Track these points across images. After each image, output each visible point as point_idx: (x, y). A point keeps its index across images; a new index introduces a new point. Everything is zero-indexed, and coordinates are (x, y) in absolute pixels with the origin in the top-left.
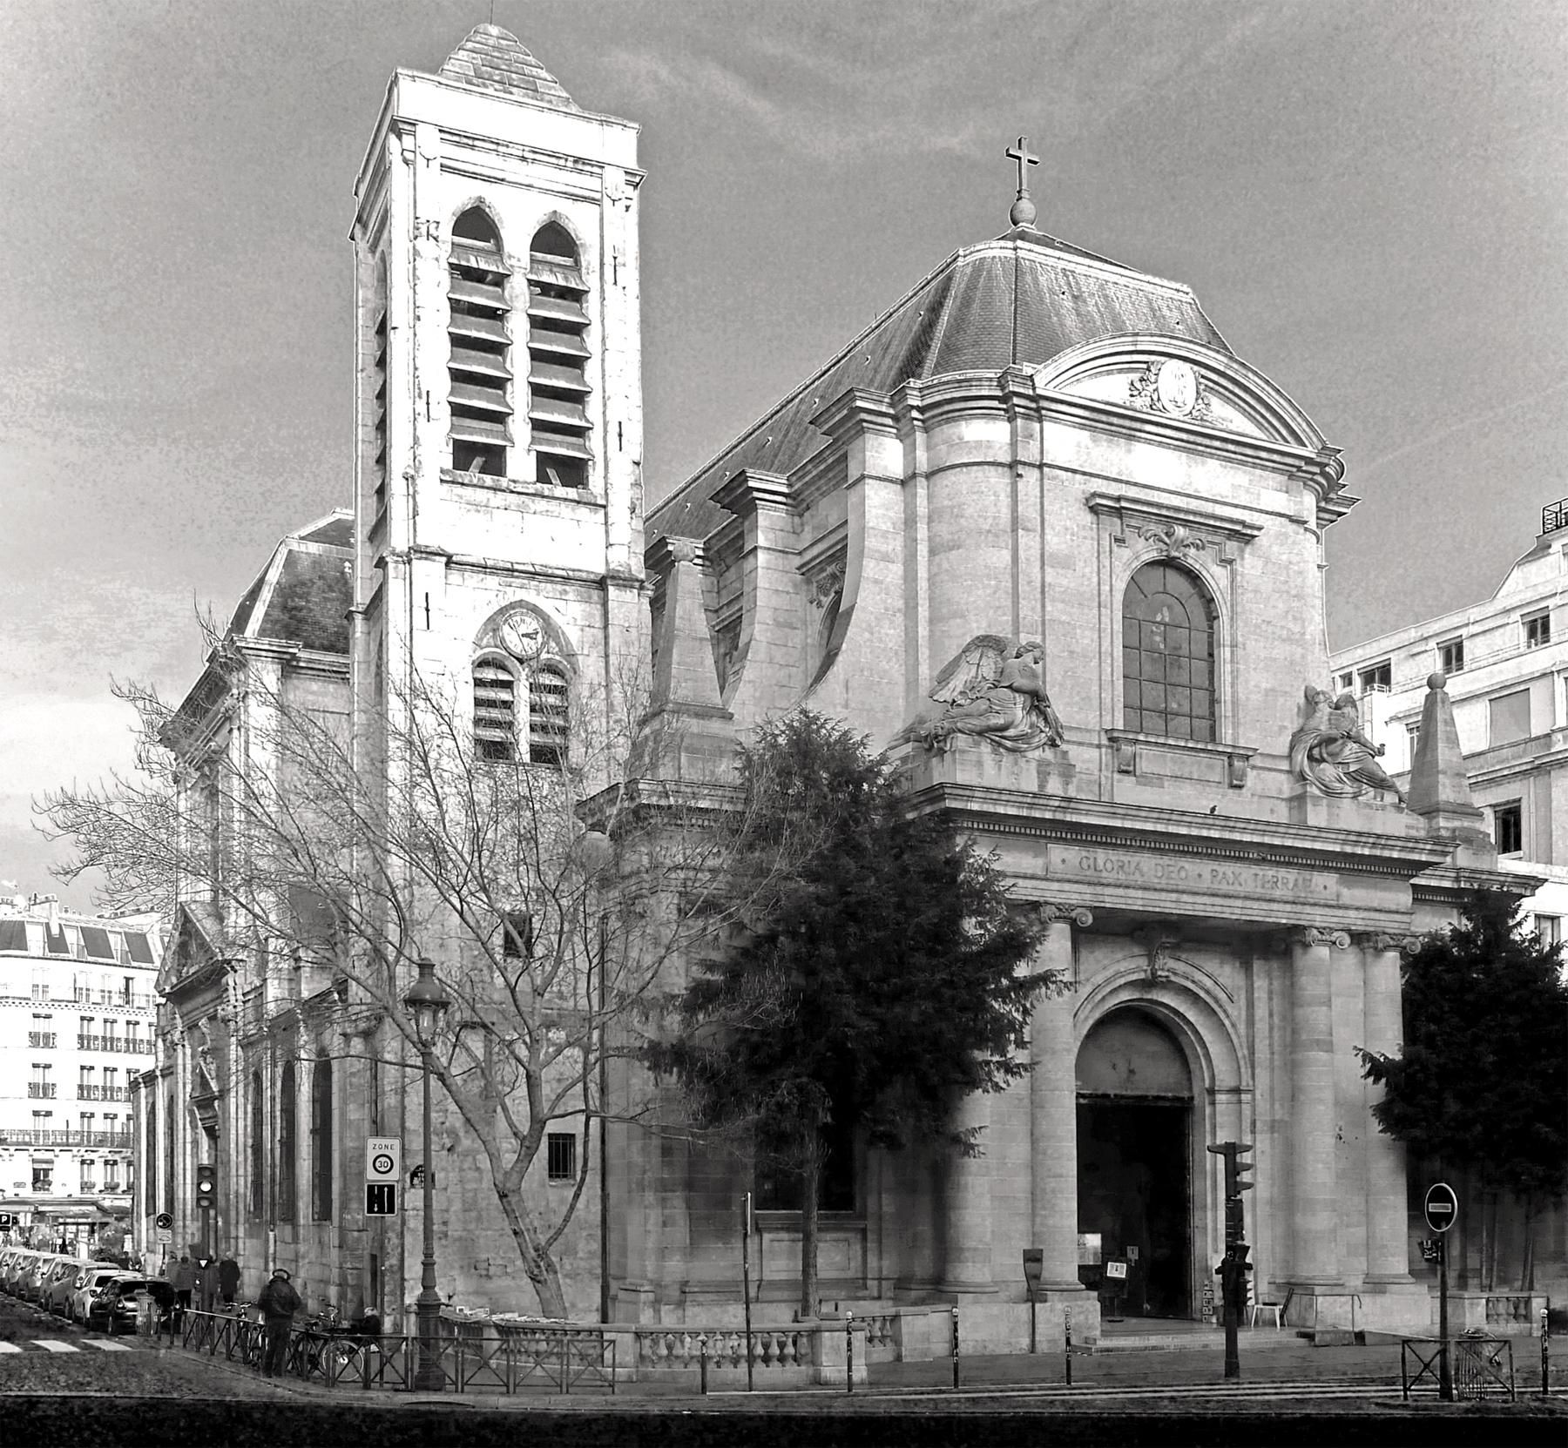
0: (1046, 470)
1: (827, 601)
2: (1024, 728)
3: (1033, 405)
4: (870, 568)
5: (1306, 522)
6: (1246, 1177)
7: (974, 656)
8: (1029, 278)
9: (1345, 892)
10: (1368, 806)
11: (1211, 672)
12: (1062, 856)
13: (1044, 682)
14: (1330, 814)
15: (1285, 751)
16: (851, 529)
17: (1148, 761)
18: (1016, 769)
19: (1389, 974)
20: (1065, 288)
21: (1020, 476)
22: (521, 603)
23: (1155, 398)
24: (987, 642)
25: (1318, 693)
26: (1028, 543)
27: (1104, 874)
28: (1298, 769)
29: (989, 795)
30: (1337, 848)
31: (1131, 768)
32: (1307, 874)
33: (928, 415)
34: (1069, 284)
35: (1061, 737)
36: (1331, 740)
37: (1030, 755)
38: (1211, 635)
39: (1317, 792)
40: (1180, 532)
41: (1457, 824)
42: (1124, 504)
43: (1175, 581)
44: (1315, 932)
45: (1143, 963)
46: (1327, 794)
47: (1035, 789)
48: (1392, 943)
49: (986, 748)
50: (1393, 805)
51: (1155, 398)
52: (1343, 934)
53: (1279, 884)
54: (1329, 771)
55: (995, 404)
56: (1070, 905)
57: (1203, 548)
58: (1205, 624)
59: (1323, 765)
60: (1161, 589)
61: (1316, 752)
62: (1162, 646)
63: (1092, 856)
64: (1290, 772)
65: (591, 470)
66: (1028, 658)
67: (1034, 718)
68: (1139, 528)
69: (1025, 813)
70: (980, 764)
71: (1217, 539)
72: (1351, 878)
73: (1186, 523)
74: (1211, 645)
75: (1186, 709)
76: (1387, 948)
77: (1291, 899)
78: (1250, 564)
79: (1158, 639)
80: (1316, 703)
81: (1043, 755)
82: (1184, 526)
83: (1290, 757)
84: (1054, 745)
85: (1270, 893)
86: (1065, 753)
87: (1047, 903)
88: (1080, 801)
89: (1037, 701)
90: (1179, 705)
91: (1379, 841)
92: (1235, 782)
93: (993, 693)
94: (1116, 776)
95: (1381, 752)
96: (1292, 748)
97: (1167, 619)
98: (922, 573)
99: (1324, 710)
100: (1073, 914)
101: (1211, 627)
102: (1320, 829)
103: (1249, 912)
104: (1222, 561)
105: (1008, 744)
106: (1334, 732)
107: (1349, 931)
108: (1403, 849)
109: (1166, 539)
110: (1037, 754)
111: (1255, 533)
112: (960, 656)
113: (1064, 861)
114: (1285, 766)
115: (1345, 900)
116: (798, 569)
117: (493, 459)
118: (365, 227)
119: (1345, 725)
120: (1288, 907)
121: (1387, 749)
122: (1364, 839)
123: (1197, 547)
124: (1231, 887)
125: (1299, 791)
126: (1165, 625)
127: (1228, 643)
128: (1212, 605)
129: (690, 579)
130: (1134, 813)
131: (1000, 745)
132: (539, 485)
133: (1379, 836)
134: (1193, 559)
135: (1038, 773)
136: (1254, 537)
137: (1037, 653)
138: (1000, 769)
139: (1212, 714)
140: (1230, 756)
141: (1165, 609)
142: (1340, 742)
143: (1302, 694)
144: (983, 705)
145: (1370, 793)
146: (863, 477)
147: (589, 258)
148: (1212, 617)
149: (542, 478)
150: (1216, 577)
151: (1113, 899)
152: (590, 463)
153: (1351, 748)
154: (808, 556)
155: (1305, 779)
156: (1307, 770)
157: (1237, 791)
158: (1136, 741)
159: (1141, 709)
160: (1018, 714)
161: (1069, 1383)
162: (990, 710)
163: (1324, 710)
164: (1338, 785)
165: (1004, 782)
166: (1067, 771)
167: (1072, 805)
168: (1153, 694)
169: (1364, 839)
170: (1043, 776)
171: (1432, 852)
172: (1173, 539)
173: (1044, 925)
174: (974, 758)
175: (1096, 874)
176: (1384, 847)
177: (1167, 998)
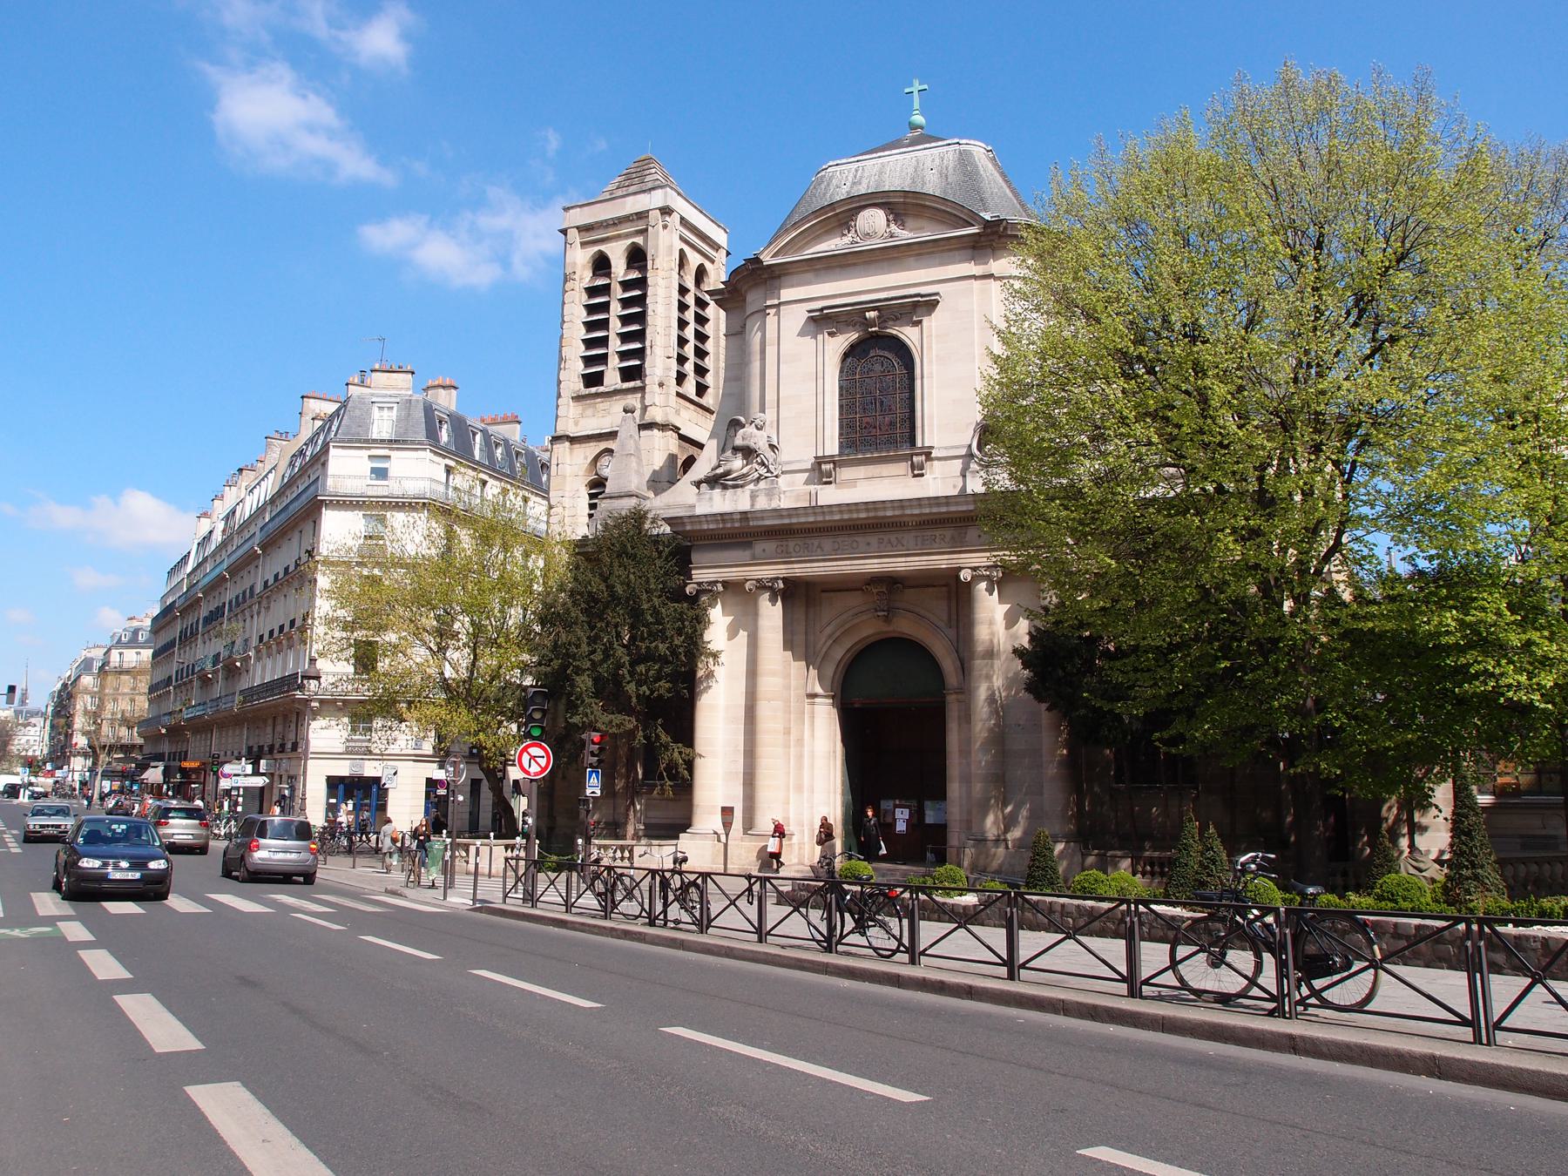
2: (745, 471)
17: (845, 473)
63: (784, 543)
73: (873, 309)
92: (916, 472)
103: (912, 564)
110: (751, 486)
150: (908, 334)
158: (834, 462)
174: (708, 496)
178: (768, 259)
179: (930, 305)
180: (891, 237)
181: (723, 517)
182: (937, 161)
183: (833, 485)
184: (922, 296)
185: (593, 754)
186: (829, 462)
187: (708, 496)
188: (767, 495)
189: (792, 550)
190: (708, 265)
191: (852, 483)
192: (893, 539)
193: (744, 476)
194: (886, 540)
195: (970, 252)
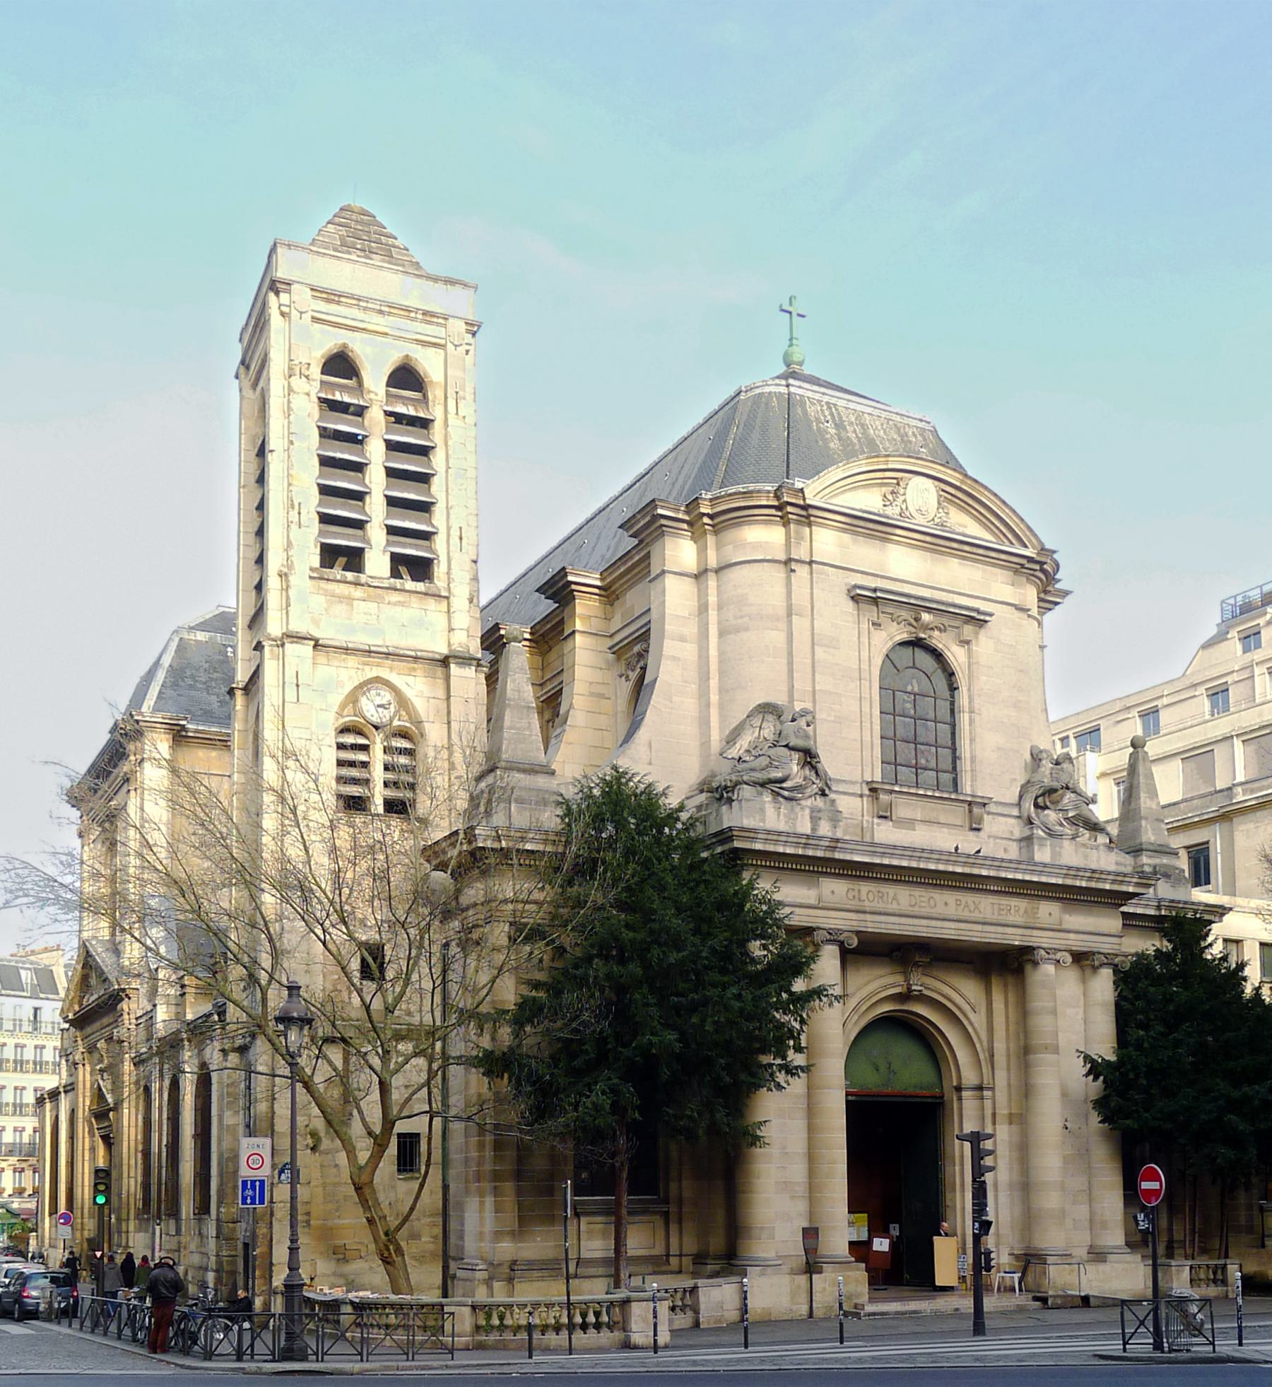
0: (814, 566)
1: (633, 675)
2: (798, 780)
3: (804, 513)
4: (670, 648)
5: (1029, 610)
6: (988, 1161)
7: (757, 722)
8: (799, 411)
9: (1067, 917)
10: (1084, 845)
11: (953, 734)
12: (835, 889)
13: (815, 742)
14: (1053, 852)
15: (1015, 799)
16: (654, 615)
17: (904, 809)
19: (1103, 986)
20: (829, 417)
21: (793, 571)
22: (378, 680)
23: (904, 507)
24: (768, 709)
25: (1041, 752)
26: (800, 624)
27: (867, 903)
28: (1025, 815)
29: (770, 837)
30: (1060, 881)
31: (889, 814)
32: (1035, 903)
33: (717, 521)
34: (832, 414)
35: (830, 788)
36: (1052, 791)
37: (803, 803)
38: (952, 703)
39: (1042, 834)
40: (926, 617)
41: (1157, 861)
42: (879, 594)
43: (921, 656)
44: (1043, 952)
45: (899, 979)
46: (1050, 835)
47: (809, 832)
48: (1106, 961)
49: (767, 798)
50: (1105, 845)
51: (904, 507)
52: (1067, 954)
53: (1012, 911)
54: (1051, 816)
55: (773, 512)
56: (838, 930)
57: (945, 631)
58: (947, 694)
59: (1046, 812)
61: (1040, 800)
62: (912, 712)
63: (856, 887)
65: (436, 569)
66: (802, 722)
67: (807, 772)
69: (800, 852)
70: (762, 810)
71: (957, 623)
73: (929, 610)
74: (952, 711)
75: (933, 765)
76: (1101, 965)
77: (1022, 924)
78: (984, 644)
80: (1040, 760)
81: (815, 803)
82: (929, 612)
83: (1019, 805)
84: (823, 794)
85: (1002, 919)
86: (833, 801)
87: (819, 928)
88: (845, 841)
89: (809, 757)
90: (927, 761)
91: (1094, 875)
92: (974, 826)
93: (772, 752)
94: (876, 820)
95: (1094, 801)
96: (1021, 797)
97: (916, 690)
98: (713, 652)
99: (1047, 766)
100: (841, 938)
101: (953, 696)
102: (1045, 865)
103: (988, 935)
105: (786, 793)
106: (1055, 784)
108: (1114, 882)
109: (914, 624)
110: (809, 802)
111: (987, 618)
112: (745, 720)
114: (1015, 812)
115: (1065, 926)
116: (610, 649)
117: (353, 559)
118: (248, 368)
119: (1064, 779)
120: (1020, 931)
121: (1099, 798)
122: (1081, 874)
123: (940, 630)
125: (1027, 833)
126: (915, 695)
127: (967, 709)
128: (953, 678)
129: (519, 657)
130: (891, 851)
131: (779, 794)
132: (392, 580)
133: (1094, 871)
134: (938, 640)
135: (811, 818)
136: (986, 622)
137: (809, 718)
138: (779, 815)
139: (954, 768)
140: (970, 803)
141: (914, 681)
142: (1060, 792)
143: (1029, 752)
144: (764, 761)
145: (1086, 834)
146: (663, 572)
147: (435, 394)
148: (953, 688)
149: (395, 574)
150: (956, 655)
151: (875, 925)
152: (435, 561)
153: (1069, 796)
154: (618, 638)
155: (1031, 823)
156: (1033, 815)
157: (976, 833)
158: (892, 792)
159: (896, 765)
160: (794, 768)
161: (842, 1343)
162: (770, 765)
163: (1047, 766)
164: (1058, 828)
165: (782, 826)
166: (835, 816)
167: (839, 845)
168: (906, 752)
169: (1081, 874)
170: (815, 820)
171: (1137, 884)
172: (920, 623)
173: (817, 947)
175: (860, 903)
180: (942, 525)
189: (864, 897)
191: (909, 824)
192: (970, 903)
194: (963, 903)
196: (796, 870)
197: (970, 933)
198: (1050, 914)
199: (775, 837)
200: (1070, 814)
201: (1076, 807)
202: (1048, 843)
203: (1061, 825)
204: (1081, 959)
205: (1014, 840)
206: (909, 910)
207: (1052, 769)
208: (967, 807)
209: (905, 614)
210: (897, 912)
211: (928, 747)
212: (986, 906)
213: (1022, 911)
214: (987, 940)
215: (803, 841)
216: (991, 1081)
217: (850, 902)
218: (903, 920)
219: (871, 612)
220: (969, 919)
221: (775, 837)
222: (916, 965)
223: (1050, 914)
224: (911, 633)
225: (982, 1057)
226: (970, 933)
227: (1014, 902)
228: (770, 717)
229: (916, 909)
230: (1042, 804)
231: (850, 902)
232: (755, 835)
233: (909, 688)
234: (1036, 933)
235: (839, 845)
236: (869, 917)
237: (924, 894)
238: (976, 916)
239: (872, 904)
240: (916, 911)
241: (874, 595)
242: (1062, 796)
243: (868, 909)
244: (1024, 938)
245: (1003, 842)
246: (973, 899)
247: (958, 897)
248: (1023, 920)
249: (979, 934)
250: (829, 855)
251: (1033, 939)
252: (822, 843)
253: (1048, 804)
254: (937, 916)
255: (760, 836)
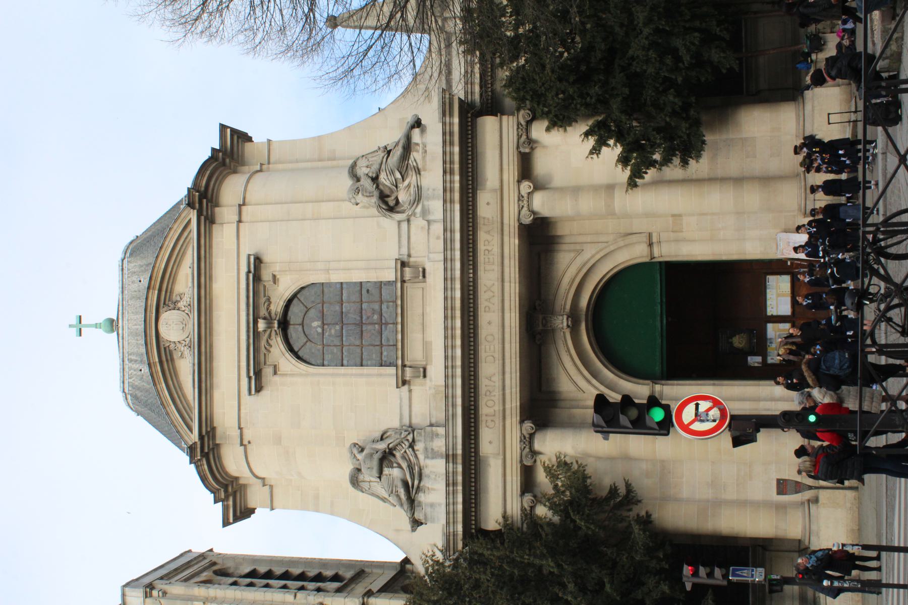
2: (404, 465)
7: (365, 486)
10: (424, 158)
17: (415, 354)
18: (433, 476)
21: (249, 442)
24: (355, 481)
29: (451, 520)
30: (457, 207)
32: (480, 221)
36: (383, 197)
40: (261, 325)
42: (252, 374)
49: (422, 497)
52: (522, 187)
53: (490, 248)
54: (403, 197)
56: (521, 437)
60: (300, 328)
64: (408, 221)
68: (265, 355)
69: (460, 488)
70: (432, 505)
71: (262, 288)
72: (479, 179)
73: (255, 322)
77: (499, 236)
78: (274, 259)
79: (333, 331)
82: (257, 322)
85: (497, 260)
87: (521, 461)
89: (386, 458)
97: (319, 323)
100: (527, 436)
104: (275, 283)
105: (416, 482)
106: (376, 193)
107: (519, 182)
110: (421, 457)
113: (490, 442)
115: (497, 184)
120: (506, 239)
123: (269, 305)
124: (496, 294)
126: (323, 324)
130: (450, 399)
131: (418, 487)
134: (277, 307)
135: (433, 458)
137: (355, 451)
138: (433, 489)
140: (403, 282)
145: (416, 156)
151: (514, 403)
158: (404, 366)
164: (412, 189)
165: (442, 486)
167: (451, 453)
169: (448, 185)
176: (452, 162)
177: (584, 302)
178: (192, 436)
179: (258, 260)
181: (450, 483)
182: (135, 278)
183: (429, 368)
184: (249, 272)
185: (710, 575)
186: (403, 372)
187: (429, 510)
188: (432, 440)
190: (215, 568)
191: (426, 346)
193: (411, 467)
194: (487, 304)
195: (215, 227)
196: (475, 469)
197: (513, 295)
198: (488, 204)
199: (451, 516)
200: (398, 175)
201: (392, 173)
202: (426, 203)
203: (409, 186)
204: (526, 169)
205: (429, 229)
206: (498, 362)
207: (363, 195)
208: (405, 285)
209: (263, 342)
210: (501, 377)
211: (363, 312)
212: (488, 278)
213: (489, 237)
214: (517, 276)
215: (451, 488)
216: (643, 235)
217: (497, 425)
218: (507, 369)
219: (267, 371)
220: (500, 298)
221: (451, 516)
222: (546, 322)
223: (488, 204)
224: (277, 334)
225: (621, 244)
226: (513, 298)
227: (481, 247)
228: (361, 477)
229: (496, 355)
230: (394, 202)
231: (497, 422)
232: (452, 534)
233: (320, 330)
234: (506, 221)
235: (451, 453)
236: (508, 406)
237: (483, 347)
238: (496, 288)
239: (497, 402)
240: (498, 355)
241: (253, 377)
242: (384, 185)
243: (501, 408)
244: (512, 234)
245: (431, 240)
246: (482, 293)
247: (483, 309)
248: (496, 235)
249: (513, 285)
250: (460, 460)
251: (512, 223)
252: (451, 470)
253: (393, 198)
254: (500, 333)
255: (451, 530)
